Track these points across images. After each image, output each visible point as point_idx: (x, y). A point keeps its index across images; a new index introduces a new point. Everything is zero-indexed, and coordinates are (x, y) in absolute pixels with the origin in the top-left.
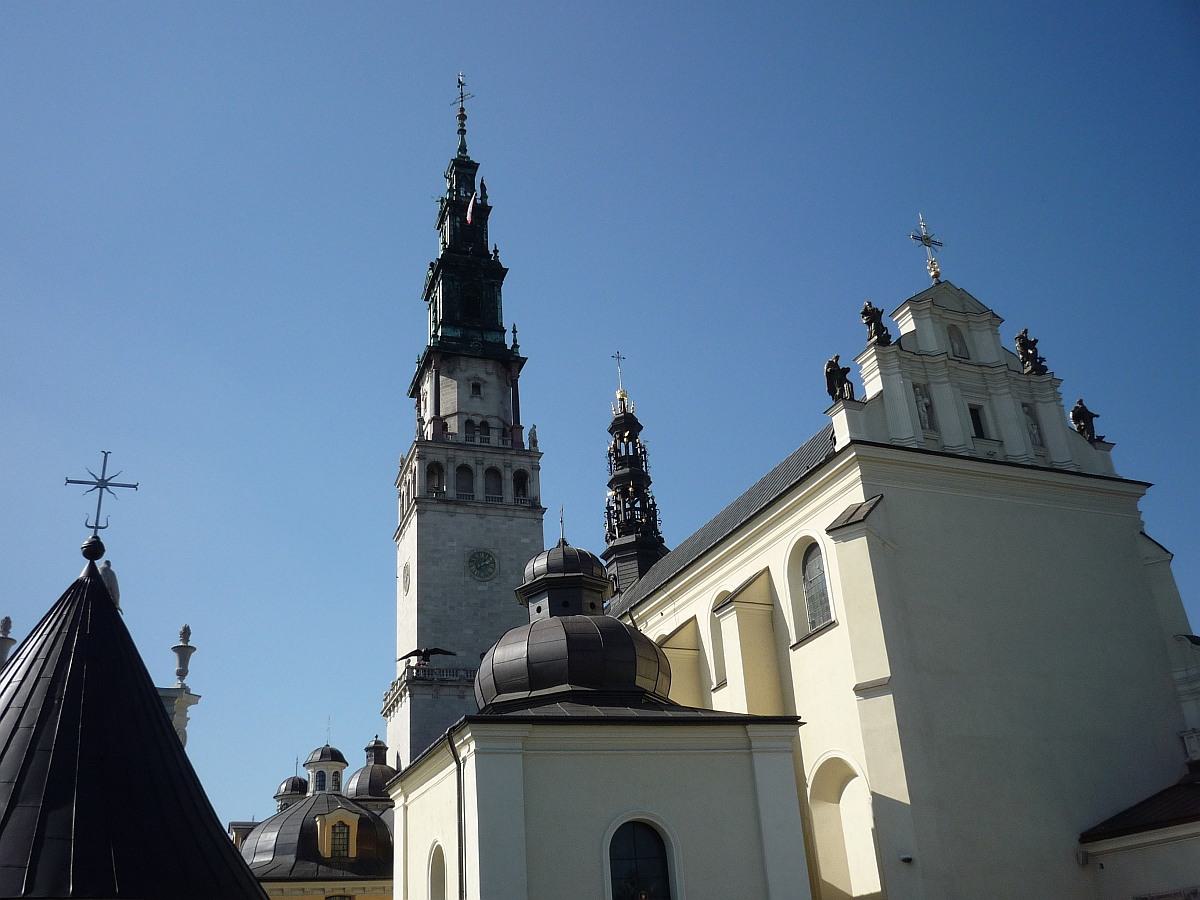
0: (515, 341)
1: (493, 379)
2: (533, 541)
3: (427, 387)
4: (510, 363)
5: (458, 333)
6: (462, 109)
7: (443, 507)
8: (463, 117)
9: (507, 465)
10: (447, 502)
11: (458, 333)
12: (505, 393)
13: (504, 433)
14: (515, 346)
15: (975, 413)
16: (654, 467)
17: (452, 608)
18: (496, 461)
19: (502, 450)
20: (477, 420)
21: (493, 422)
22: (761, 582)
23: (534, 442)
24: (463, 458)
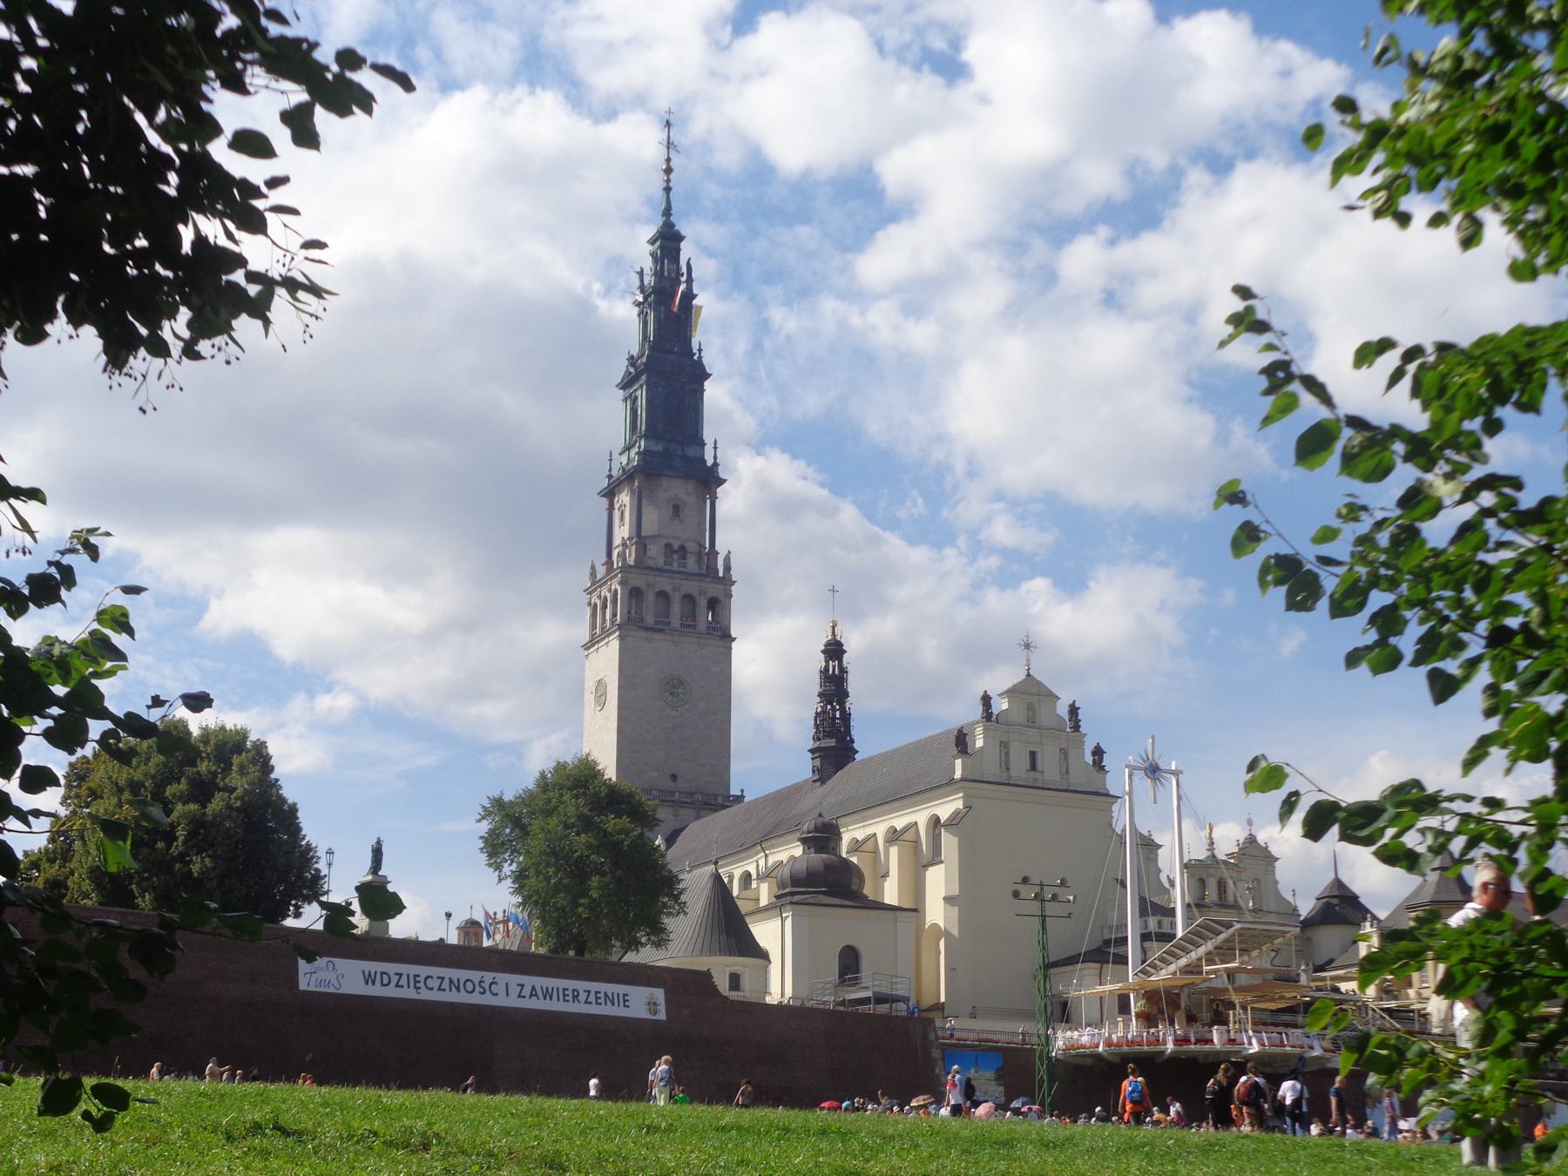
3: (624, 498)
4: (708, 480)
5: (659, 447)
6: (668, 160)
7: (642, 634)
8: (668, 171)
9: (701, 592)
10: (647, 629)
11: (658, 447)
13: (699, 555)
14: (716, 464)
15: (1033, 754)
16: (853, 684)
18: (692, 587)
20: (676, 544)
21: (691, 547)
22: (912, 831)
23: (728, 568)
24: (663, 583)
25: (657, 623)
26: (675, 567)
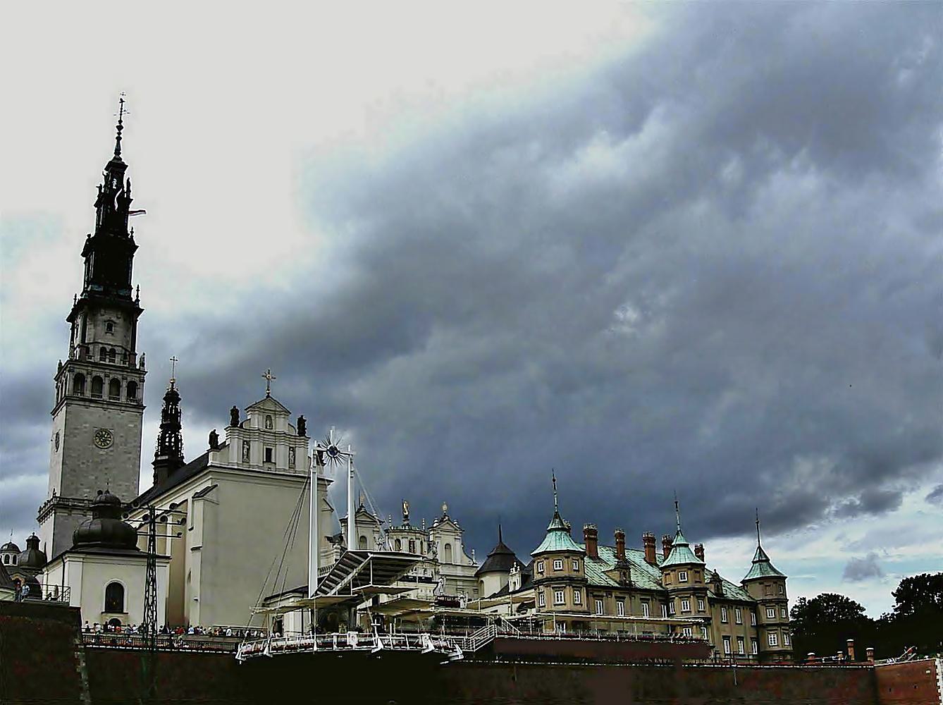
0: (137, 296)
1: (120, 321)
2: (135, 426)
3: (79, 321)
4: (132, 311)
6: (120, 122)
8: (120, 128)
14: (138, 300)
15: (269, 451)
17: (83, 463)
20: (108, 348)
21: (118, 350)
23: (142, 364)
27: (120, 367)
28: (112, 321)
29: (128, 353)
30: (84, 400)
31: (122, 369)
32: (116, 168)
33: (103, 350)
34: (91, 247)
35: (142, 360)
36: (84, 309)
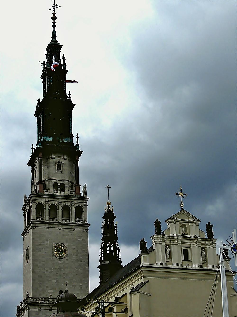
0: (77, 142)
1: (66, 162)
2: (83, 240)
3: (37, 164)
6: (54, 14)
7: (43, 225)
8: (54, 18)
12: (72, 167)
13: (72, 188)
14: (78, 145)
17: (47, 271)
19: (70, 198)
20: (59, 183)
21: (67, 184)
23: (85, 193)
24: (53, 201)
25: (50, 219)
26: (59, 193)
27: (69, 196)
28: (60, 162)
29: (74, 185)
30: (45, 223)
31: (70, 198)
32: (54, 49)
33: (56, 185)
34: (41, 108)
35: (85, 189)
36: (39, 156)
